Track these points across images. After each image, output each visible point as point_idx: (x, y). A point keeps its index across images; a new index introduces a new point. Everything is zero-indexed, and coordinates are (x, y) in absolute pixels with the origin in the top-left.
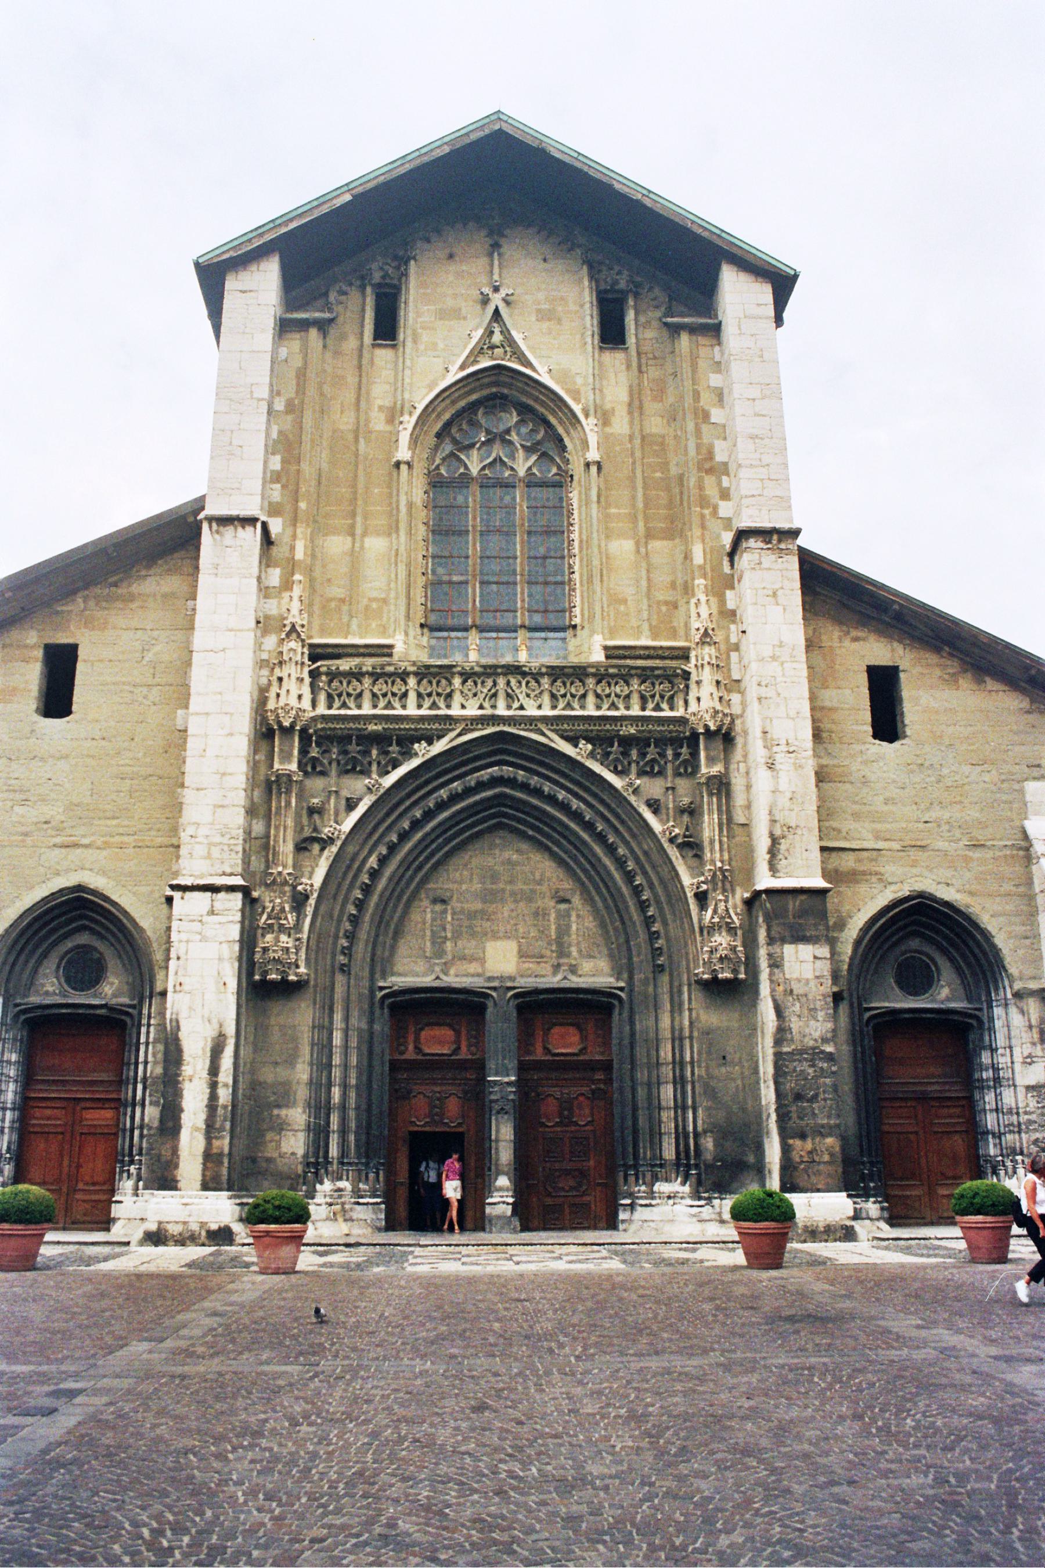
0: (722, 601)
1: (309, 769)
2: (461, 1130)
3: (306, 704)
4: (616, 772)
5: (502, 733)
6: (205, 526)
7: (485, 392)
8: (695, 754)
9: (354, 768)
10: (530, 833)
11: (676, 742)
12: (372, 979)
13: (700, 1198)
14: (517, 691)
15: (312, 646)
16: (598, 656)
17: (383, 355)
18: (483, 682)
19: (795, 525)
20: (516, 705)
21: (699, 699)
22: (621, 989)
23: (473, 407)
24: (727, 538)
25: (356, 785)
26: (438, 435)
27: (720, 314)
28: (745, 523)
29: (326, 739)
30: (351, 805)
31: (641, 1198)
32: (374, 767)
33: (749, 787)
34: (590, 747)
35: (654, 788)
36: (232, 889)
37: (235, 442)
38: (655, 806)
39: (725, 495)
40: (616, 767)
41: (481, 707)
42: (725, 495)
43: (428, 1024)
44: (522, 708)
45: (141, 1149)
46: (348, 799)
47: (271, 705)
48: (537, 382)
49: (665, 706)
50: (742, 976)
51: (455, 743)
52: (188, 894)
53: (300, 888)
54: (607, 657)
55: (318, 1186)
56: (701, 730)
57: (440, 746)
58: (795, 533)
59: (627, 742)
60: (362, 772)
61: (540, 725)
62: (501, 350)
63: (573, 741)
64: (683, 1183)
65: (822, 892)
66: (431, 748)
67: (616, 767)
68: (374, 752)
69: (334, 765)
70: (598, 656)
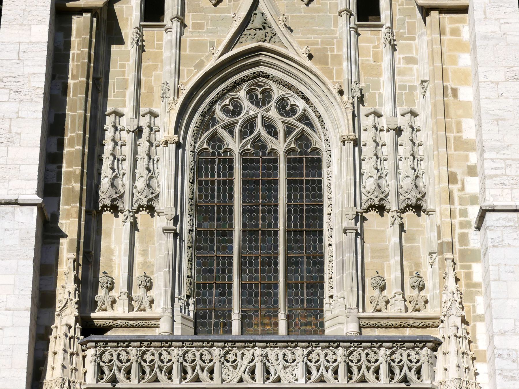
18: (243, 354)
24: (474, 212)
28: (487, 204)
37: (14, 130)
41: (241, 380)
54: (360, 328)
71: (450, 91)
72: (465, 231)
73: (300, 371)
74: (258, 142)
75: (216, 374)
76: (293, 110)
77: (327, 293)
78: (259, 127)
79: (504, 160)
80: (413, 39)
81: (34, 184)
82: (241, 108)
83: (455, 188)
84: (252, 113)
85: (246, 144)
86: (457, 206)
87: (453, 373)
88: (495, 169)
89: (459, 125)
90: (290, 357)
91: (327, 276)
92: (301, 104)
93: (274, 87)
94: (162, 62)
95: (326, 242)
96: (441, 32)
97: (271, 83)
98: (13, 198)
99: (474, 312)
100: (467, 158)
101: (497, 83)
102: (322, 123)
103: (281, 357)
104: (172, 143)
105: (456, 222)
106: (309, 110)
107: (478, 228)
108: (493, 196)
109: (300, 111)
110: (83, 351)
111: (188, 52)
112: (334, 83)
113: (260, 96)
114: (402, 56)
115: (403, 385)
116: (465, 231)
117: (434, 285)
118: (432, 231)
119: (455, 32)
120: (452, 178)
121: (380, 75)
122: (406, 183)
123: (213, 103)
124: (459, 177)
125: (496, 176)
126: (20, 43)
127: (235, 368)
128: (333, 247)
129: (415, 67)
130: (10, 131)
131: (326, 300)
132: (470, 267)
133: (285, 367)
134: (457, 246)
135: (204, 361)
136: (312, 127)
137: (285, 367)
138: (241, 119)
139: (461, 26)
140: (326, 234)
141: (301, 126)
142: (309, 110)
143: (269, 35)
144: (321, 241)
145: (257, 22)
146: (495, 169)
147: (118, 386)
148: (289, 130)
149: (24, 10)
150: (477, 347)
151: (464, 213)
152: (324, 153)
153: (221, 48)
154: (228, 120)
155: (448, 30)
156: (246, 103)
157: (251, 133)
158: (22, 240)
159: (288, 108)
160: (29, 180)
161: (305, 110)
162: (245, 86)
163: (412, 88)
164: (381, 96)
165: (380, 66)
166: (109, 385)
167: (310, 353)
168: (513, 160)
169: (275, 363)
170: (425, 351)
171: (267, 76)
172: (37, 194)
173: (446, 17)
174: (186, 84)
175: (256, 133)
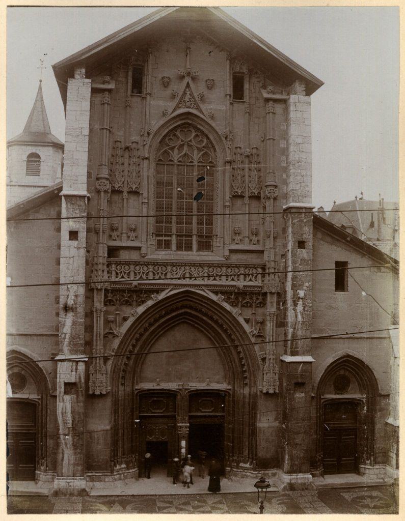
2: (165, 440)
5: (188, 290)
6: (63, 198)
7: (183, 122)
8: (265, 299)
9: (128, 303)
10: (196, 325)
11: (259, 294)
12: (133, 386)
13: (256, 471)
17: (136, 100)
22: (230, 389)
23: (175, 128)
25: (127, 311)
26: (160, 142)
29: (114, 291)
30: (125, 319)
31: (235, 468)
35: (248, 313)
38: (247, 321)
48: (202, 119)
49: (253, 279)
50: (277, 391)
51: (168, 295)
55: (115, 468)
57: (162, 296)
61: (203, 288)
62: (189, 103)
63: (216, 293)
64: (250, 465)
65: (311, 363)
66: (158, 296)
67: (233, 304)
68: (135, 297)
93: (193, 131)
153: (171, 111)
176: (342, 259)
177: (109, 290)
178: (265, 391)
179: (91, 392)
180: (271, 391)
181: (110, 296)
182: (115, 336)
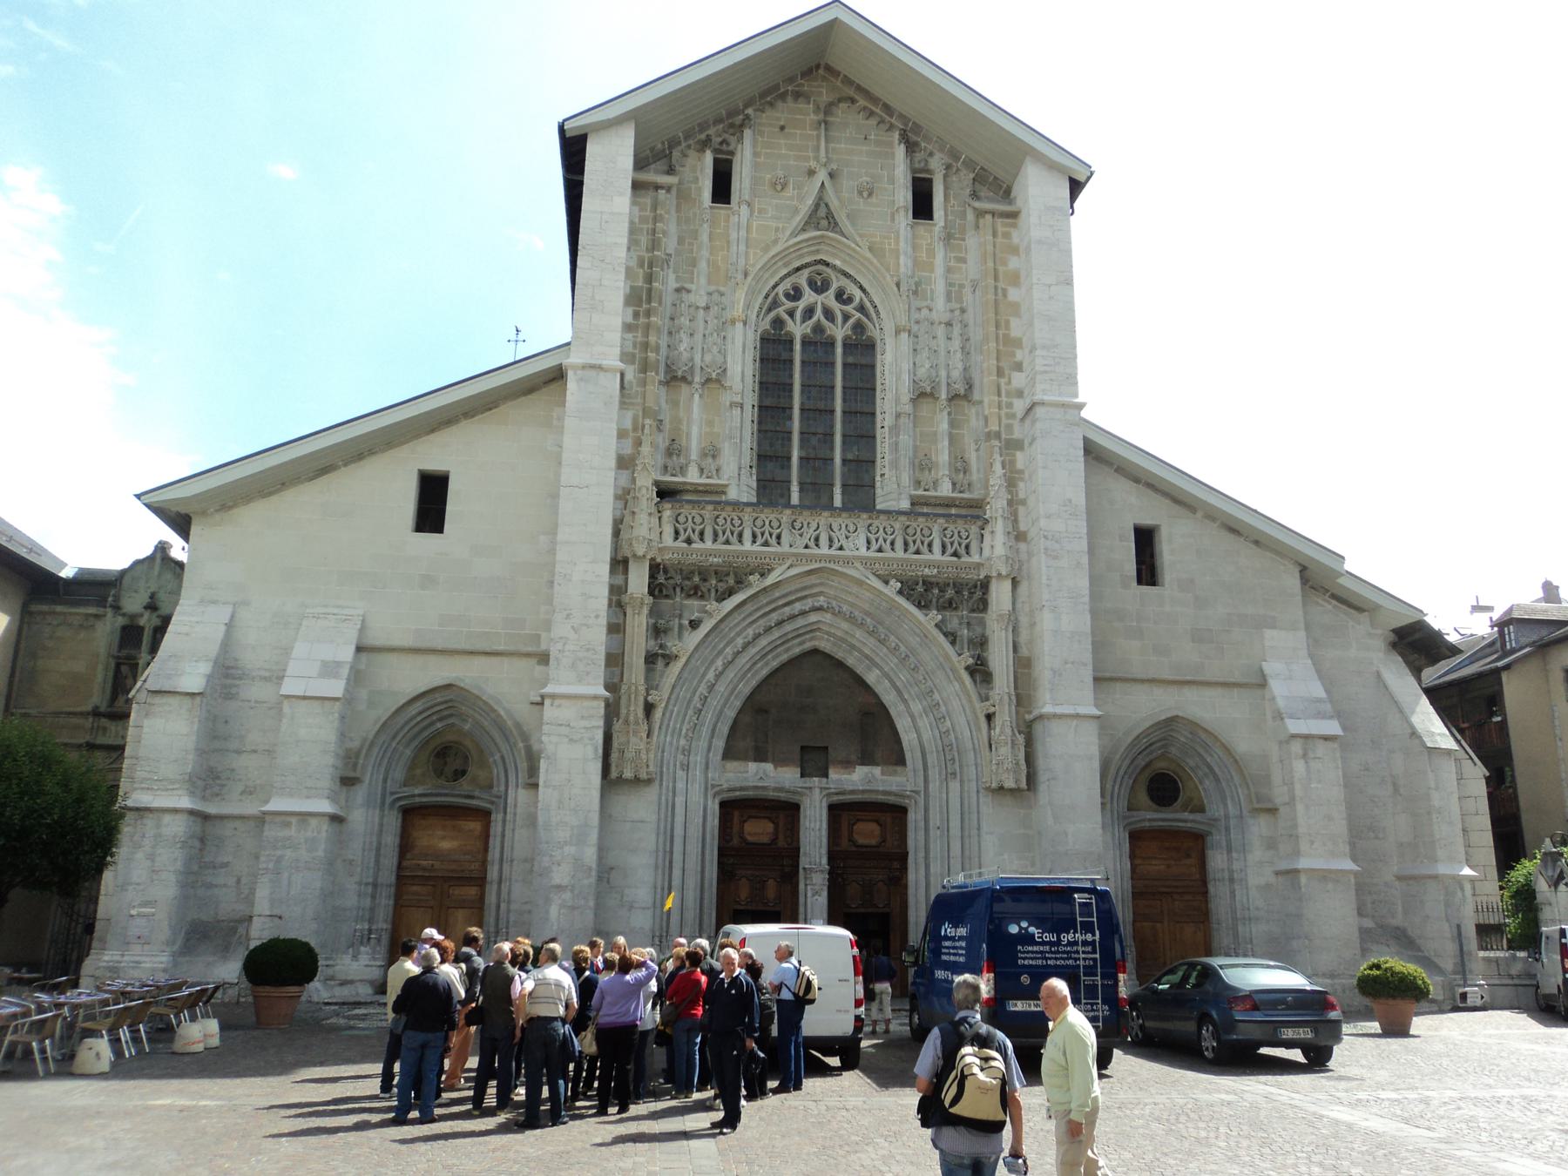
0: (1013, 462)
1: (656, 593)
3: (654, 536)
4: (919, 606)
9: (695, 592)
14: (838, 533)
15: (657, 483)
16: (905, 505)
19: (1080, 400)
20: (836, 545)
21: (992, 547)
22: (917, 792)
27: (1019, 203)
28: (1037, 398)
30: (694, 625)
32: (713, 594)
33: (1033, 625)
34: (899, 585)
36: (595, 697)
39: (1018, 367)
40: (919, 603)
42: (1018, 367)
43: (750, 817)
44: (841, 548)
45: (508, 922)
46: (691, 622)
47: (624, 535)
52: (557, 702)
53: (649, 698)
56: (994, 574)
58: (1081, 406)
59: (928, 584)
60: (702, 597)
67: (919, 603)
69: (678, 590)
70: (905, 505)
71: (1000, 291)
72: (1010, 421)
73: (861, 542)
74: (818, 329)
75: (784, 539)
76: (850, 300)
77: (878, 473)
78: (819, 314)
79: (1054, 358)
80: (964, 240)
81: (617, 351)
82: (801, 293)
83: (1003, 381)
84: (812, 300)
85: (806, 328)
86: (1004, 399)
87: (1000, 550)
88: (1045, 365)
89: (1007, 322)
90: (852, 528)
91: (879, 456)
92: (858, 294)
94: (728, 242)
95: (879, 425)
96: (995, 235)
97: (829, 270)
98: (598, 362)
99: (1017, 495)
100: (1013, 355)
101: (1050, 286)
102: (877, 313)
103: (843, 526)
104: (739, 321)
105: (1003, 413)
106: (865, 300)
107: (1023, 419)
108: (1043, 390)
109: (857, 300)
110: (659, 512)
111: (754, 235)
112: (892, 276)
113: (819, 284)
114: (953, 255)
115: (955, 559)
116: (1010, 421)
117: (978, 470)
118: (977, 419)
119: (1007, 235)
120: (1000, 373)
121: (932, 271)
122: (956, 374)
123: (774, 287)
124: (1007, 372)
125: (1046, 372)
126: (601, 212)
127: (801, 535)
128: (886, 429)
129: (964, 266)
130: (593, 298)
131: (878, 478)
132: (1014, 455)
133: (847, 538)
134: (1003, 436)
135: (772, 528)
136: (867, 316)
137: (847, 538)
138: (802, 305)
139: (1012, 230)
140: (879, 417)
141: (858, 315)
142: (865, 300)
143: (832, 225)
144: (874, 423)
145: (822, 212)
146: (1045, 365)
147: (694, 545)
148: (846, 317)
149: (606, 181)
150: (1018, 528)
151: (1010, 405)
152: (879, 341)
153: (788, 233)
154: (789, 305)
155: (1000, 234)
156: (807, 290)
157: (810, 318)
158: (605, 404)
159: (845, 297)
160: (611, 346)
161: (861, 300)
162: (806, 273)
163: (962, 286)
164: (932, 291)
165: (932, 264)
166: (685, 545)
167: (870, 525)
168: (1061, 358)
169: (838, 533)
170: (974, 529)
171: (827, 264)
172: (621, 361)
173: (999, 221)
174: (753, 265)
175: (815, 319)
176: (1146, 521)
177: (660, 564)
178: (994, 785)
179: (614, 774)
180: (1009, 783)
181: (661, 579)
182: (669, 659)
